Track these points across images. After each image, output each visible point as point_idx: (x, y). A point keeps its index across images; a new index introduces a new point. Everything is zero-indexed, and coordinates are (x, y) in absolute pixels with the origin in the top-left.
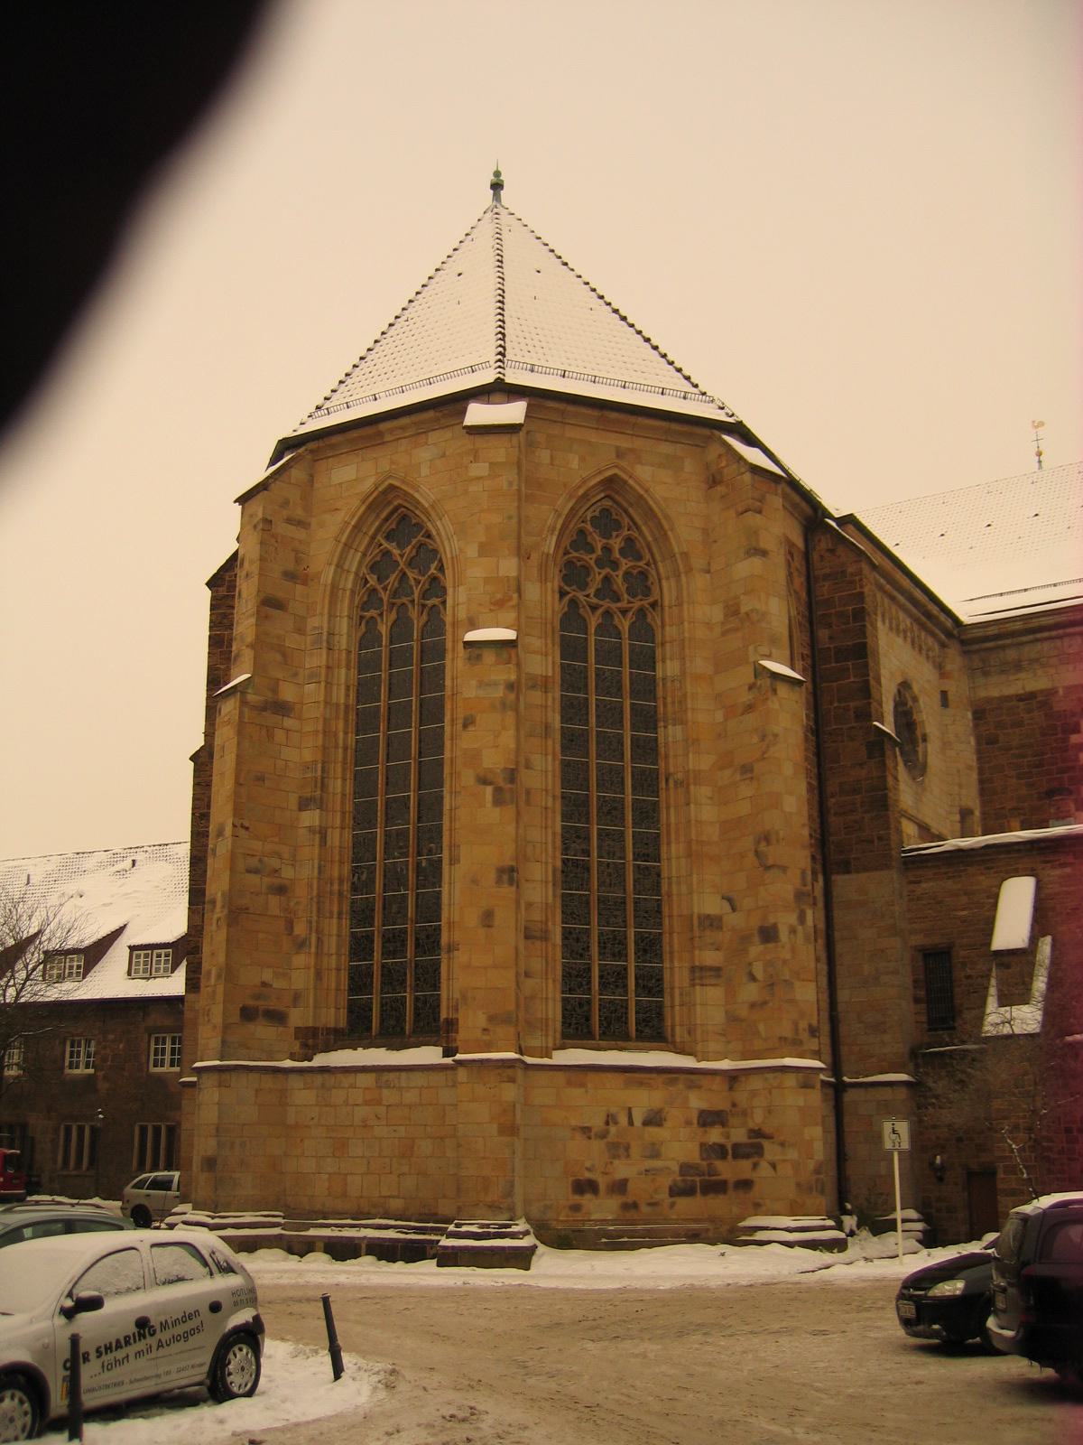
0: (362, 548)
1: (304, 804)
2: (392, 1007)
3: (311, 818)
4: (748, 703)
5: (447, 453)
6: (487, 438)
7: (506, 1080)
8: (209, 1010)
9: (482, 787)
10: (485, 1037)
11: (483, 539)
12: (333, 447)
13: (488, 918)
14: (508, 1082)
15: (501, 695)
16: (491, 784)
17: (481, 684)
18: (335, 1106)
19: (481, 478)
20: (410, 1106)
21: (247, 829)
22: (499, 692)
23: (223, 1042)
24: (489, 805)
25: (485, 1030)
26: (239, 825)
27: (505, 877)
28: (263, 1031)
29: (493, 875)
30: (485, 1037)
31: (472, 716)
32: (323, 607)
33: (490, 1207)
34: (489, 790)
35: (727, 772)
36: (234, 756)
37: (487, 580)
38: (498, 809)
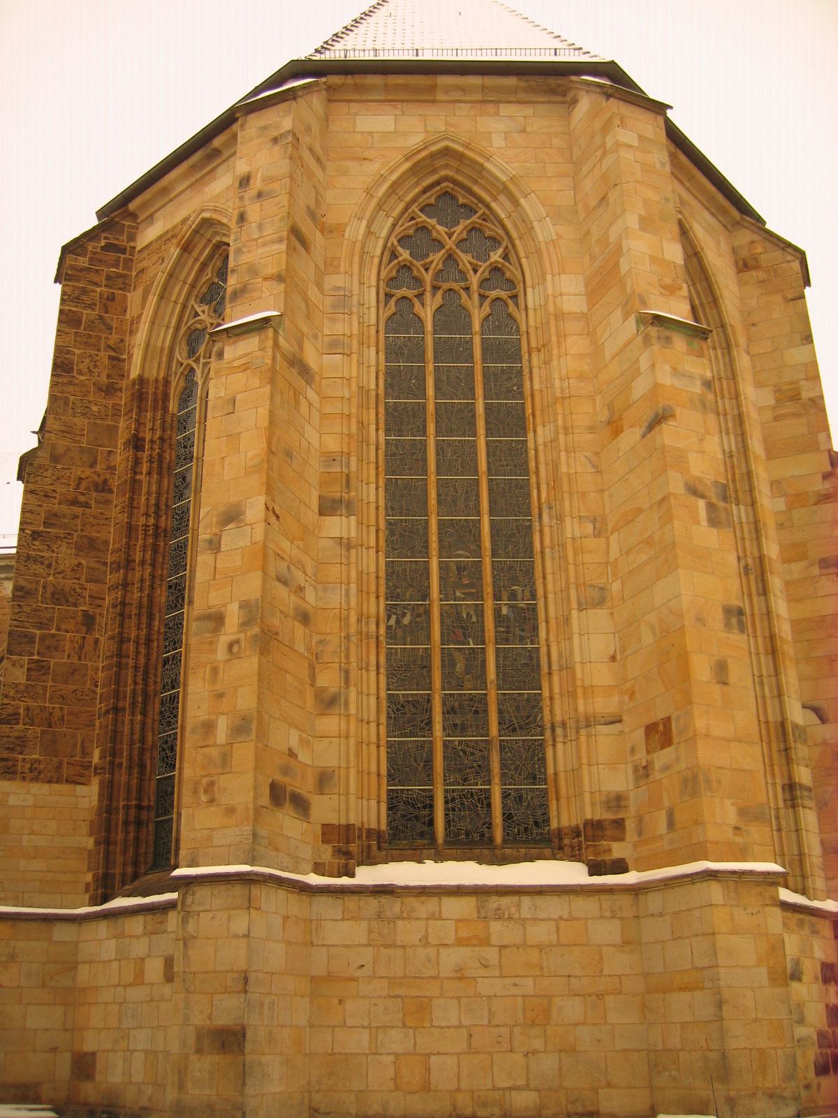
0: (396, 213)
1: (328, 507)
2: (463, 804)
3: (337, 526)
4: (824, 492)
5: (528, 129)
6: (632, 108)
7: (768, 902)
8: (212, 784)
9: (694, 498)
10: (739, 840)
11: (643, 213)
12: (358, 88)
13: (721, 669)
14: (773, 905)
15: (699, 391)
16: (702, 497)
17: (675, 372)
18: (404, 947)
19: (631, 146)
20: (540, 947)
21: (278, 517)
22: (697, 389)
23: (254, 835)
24: (704, 523)
25: (736, 828)
26: (271, 509)
27: (734, 621)
28: (288, 823)
29: (719, 615)
30: (739, 840)
31: (671, 408)
32: (351, 265)
33: (771, 1096)
34: (701, 504)
35: (802, 564)
36: (264, 411)
37: (653, 259)
38: (715, 531)
